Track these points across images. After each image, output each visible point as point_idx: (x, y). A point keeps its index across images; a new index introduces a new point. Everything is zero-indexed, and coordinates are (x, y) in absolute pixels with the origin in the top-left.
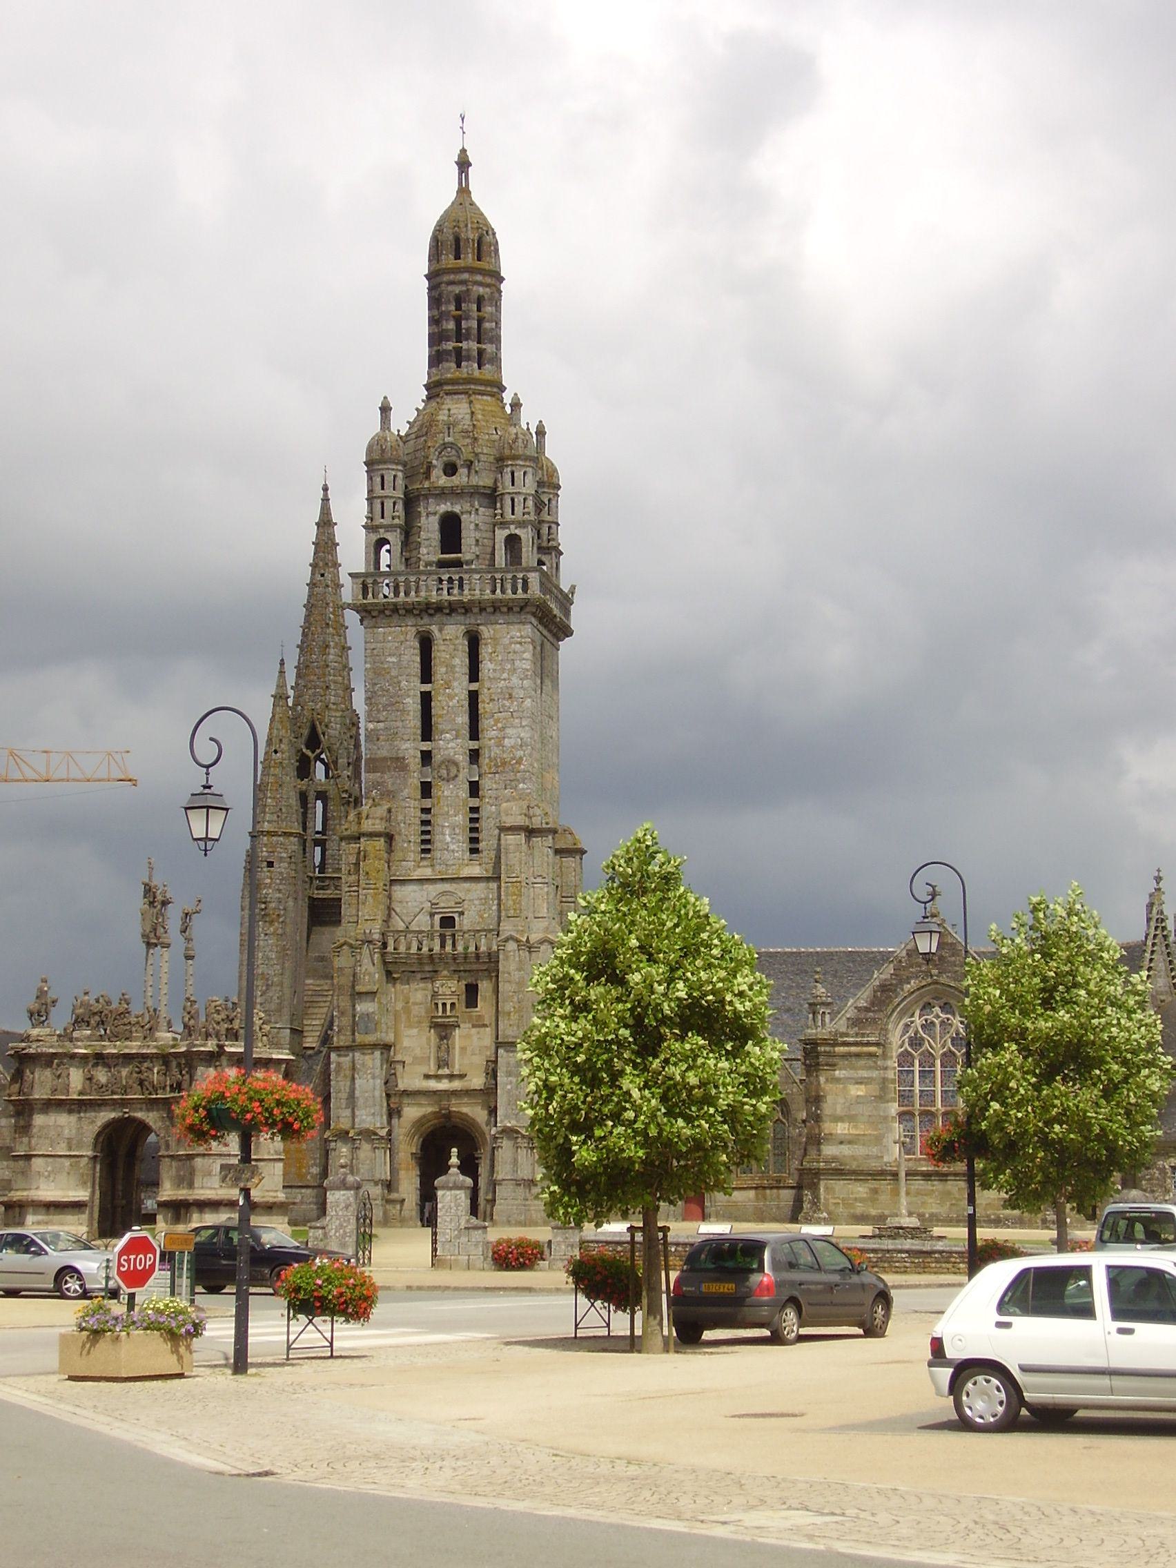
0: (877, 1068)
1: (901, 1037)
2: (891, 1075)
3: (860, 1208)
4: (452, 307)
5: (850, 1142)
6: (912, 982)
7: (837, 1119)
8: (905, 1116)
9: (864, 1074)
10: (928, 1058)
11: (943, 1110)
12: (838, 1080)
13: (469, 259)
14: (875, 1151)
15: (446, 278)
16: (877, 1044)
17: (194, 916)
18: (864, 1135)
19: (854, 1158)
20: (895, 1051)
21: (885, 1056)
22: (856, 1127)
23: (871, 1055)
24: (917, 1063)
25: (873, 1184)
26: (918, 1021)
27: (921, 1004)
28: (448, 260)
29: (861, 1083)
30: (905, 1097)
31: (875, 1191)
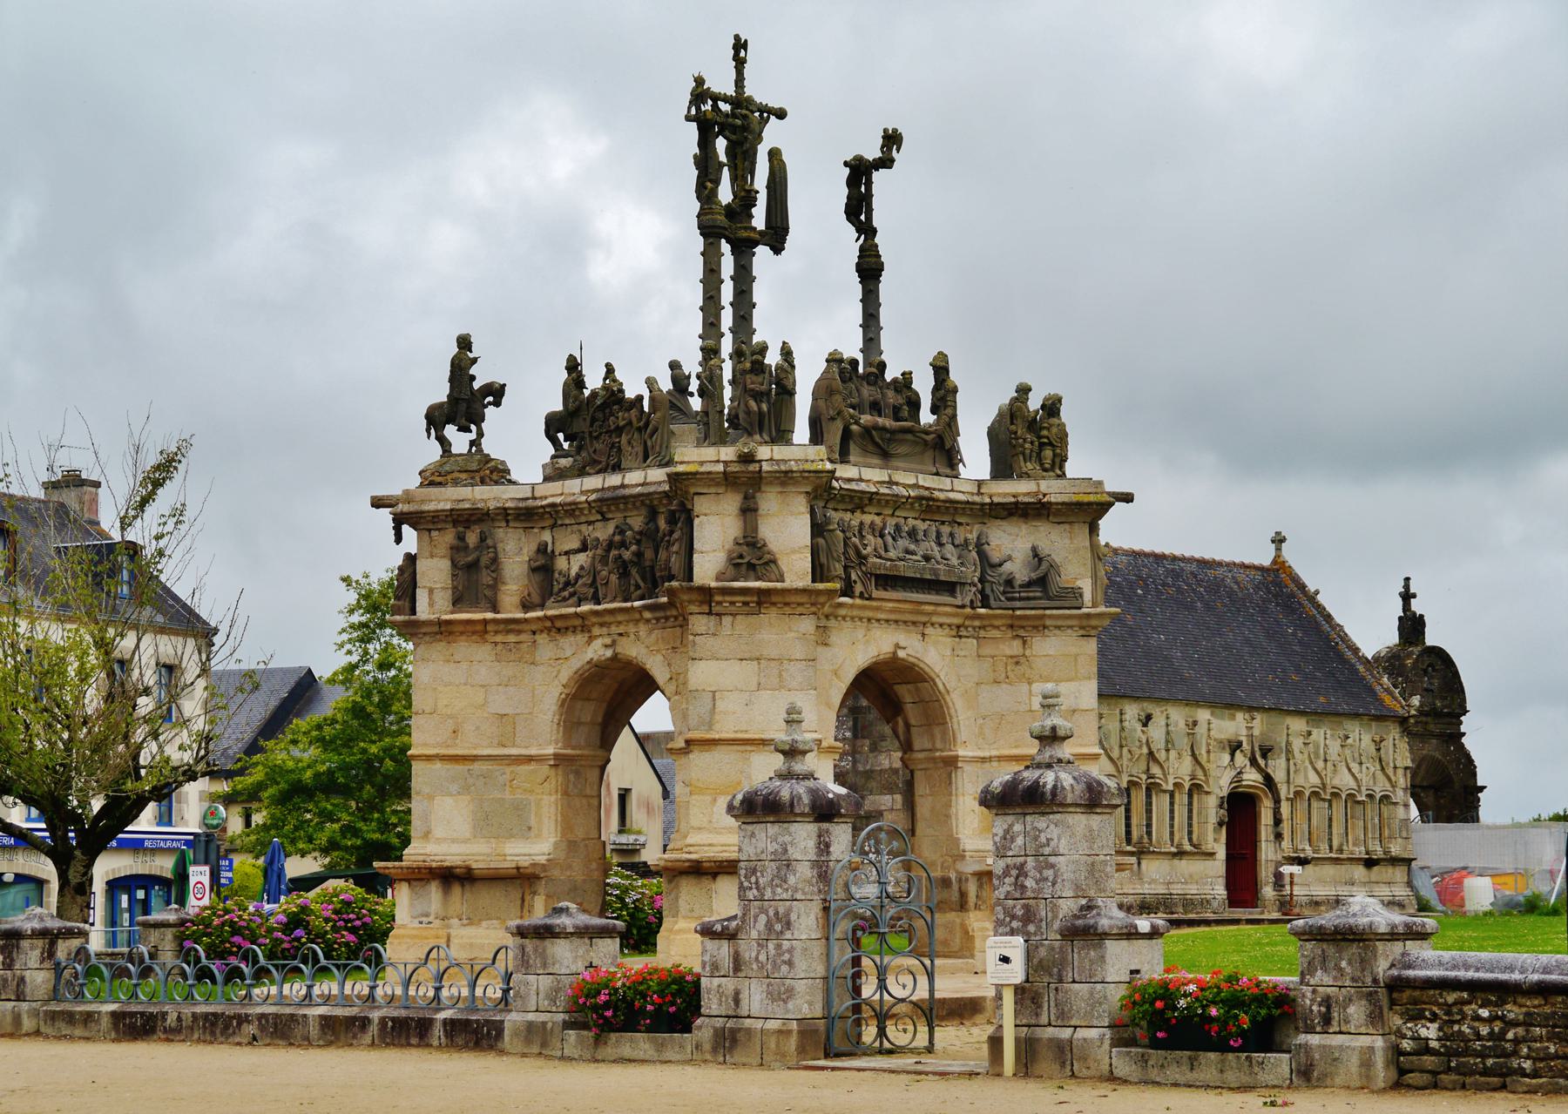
17: (878, 177)
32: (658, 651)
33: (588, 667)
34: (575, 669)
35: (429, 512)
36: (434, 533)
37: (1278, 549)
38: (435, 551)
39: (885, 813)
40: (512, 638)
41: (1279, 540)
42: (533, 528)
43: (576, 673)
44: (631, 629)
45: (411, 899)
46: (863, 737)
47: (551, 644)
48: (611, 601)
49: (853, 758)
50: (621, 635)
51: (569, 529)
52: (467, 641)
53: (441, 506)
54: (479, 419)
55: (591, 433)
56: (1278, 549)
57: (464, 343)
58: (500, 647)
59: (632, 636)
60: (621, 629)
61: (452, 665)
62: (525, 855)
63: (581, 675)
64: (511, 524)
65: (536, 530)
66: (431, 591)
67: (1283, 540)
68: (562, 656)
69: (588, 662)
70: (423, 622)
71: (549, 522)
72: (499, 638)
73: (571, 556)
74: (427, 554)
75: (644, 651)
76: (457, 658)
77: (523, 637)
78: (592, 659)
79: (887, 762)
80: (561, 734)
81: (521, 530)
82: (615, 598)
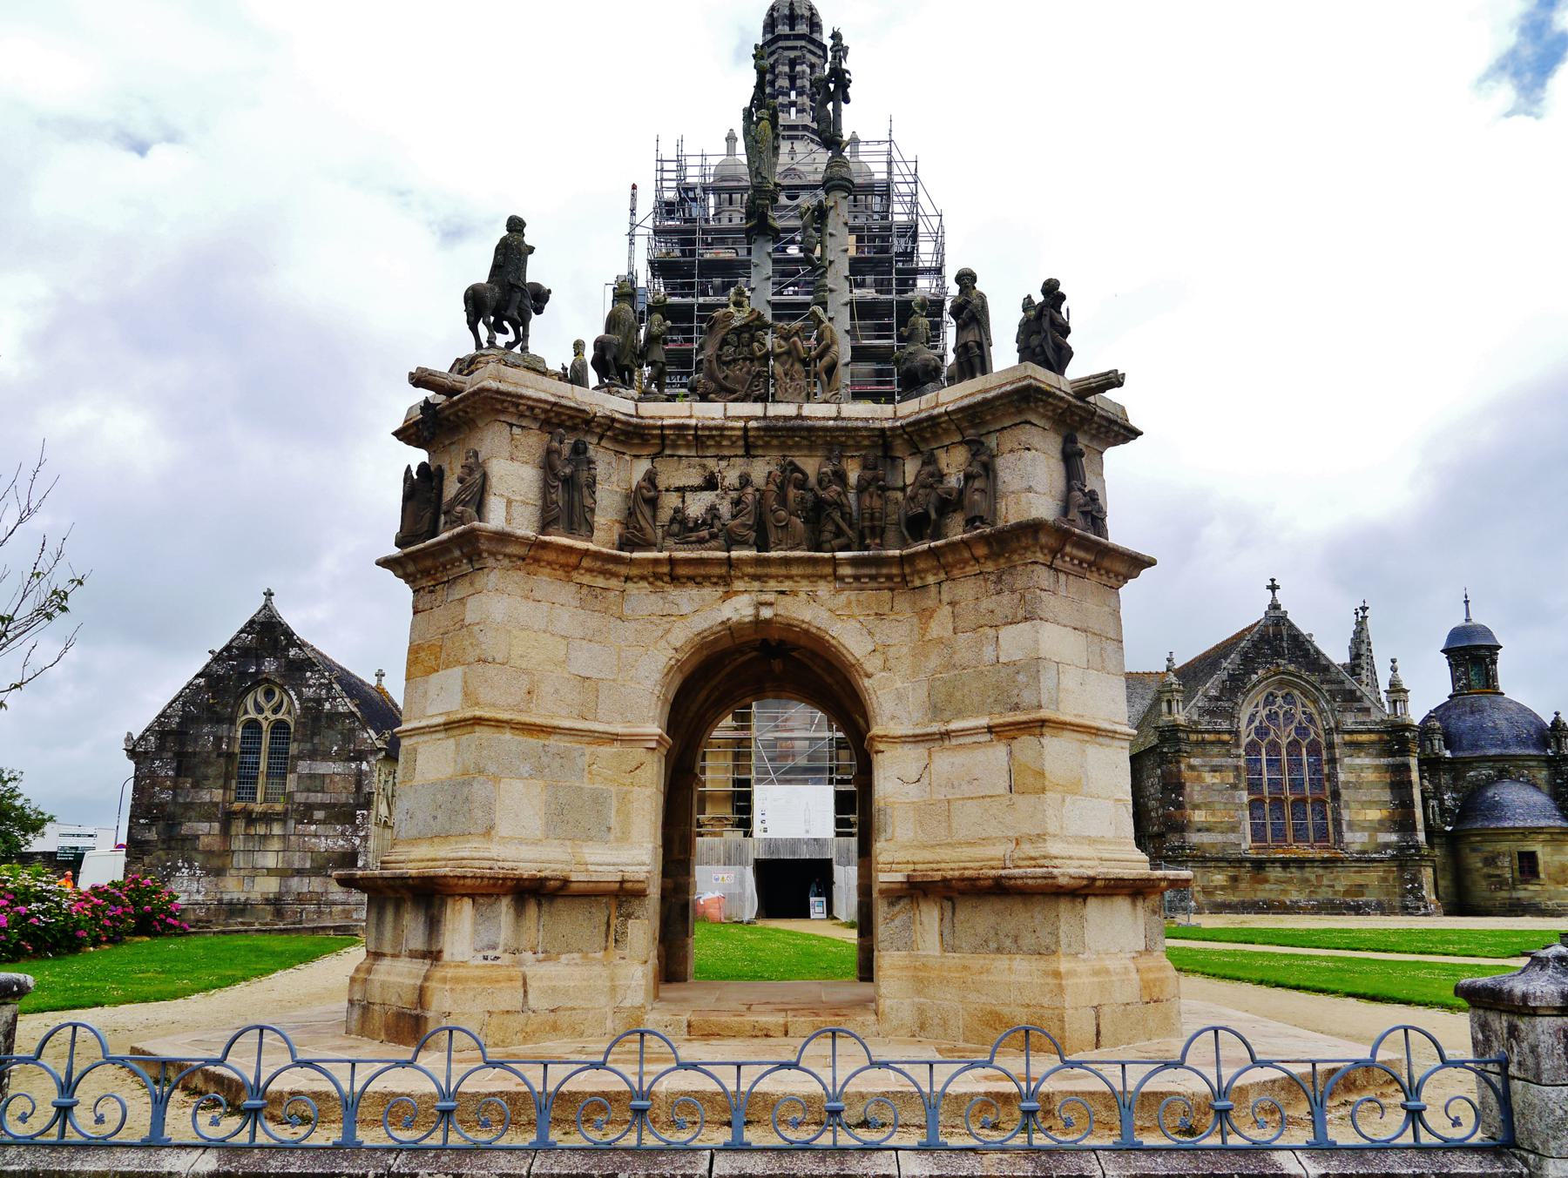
0: (1229, 755)
1: (1247, 727)
2: (1242, 763)
3: (1220, 897)
4: (787, 69)
5: (1208, 830)
6: (1260, 672)
7: (1196, 807)
8: (1255, 805)
9: (1216, 761)
10: (1274, 747)
11: (1291, 798)
12: (1191, 768)
13: (802, 28)
14: (1232, 837)
15: (781, 44)
16: (1230, 733)
18: (1222, 822)
19: (1213, 845)
20: (1244, 741)
21: (1238, 746)
22: (1213, 815)
23: (1225, 743)
24: (1264, 750)
25: (1231, 872)
26: (1264, 713)
27: (1265, 694)
28: (784, 29)
29: (1215, 771)
30: (1254, 786)
31: (1235, 879)
32: (849, 616)
33: (720, 628)
34: (696, 631)
35: (529, 398)
36: (516, 430)
37: (380, 680)
38: (516, 453)
39: (201, 837)
40: (600, 582)
41: (380, 675)
42: (624, 454)
43: (699, 634)
44: (805, 586)
45: (475, 924)
46: (186, 776)
47: (653, 597)
48: (791, 549)
49: (174, 792)
50: (782, 593)
51: (685, 461)
52: (549, 576)
53: (543, 396)
54: (521, 324)
55: (719, 357)
56: (380, 680)
57: (516, 225)
58: (585, 590)
59: (803, 596)
60: (787, 586)
61: (531, 604)
62: (609, 865)
63: (704, 638)
64: (603, 443)
65: (627, 457)
66: (509, 503)
67: (383, 675)
68: (675, 611)
69: (723, 623)
70: (517, 538)
71: (653, 450)
72: (587, 579)
73: (688, 494)
74: (507, 454)
75: (826, 615)
76: (537, 594)
77: (613, 583)
78: (728, 619)
79: (208, 796)
80: (658, 711)
81: (612, 453)
82: (798, 544)
